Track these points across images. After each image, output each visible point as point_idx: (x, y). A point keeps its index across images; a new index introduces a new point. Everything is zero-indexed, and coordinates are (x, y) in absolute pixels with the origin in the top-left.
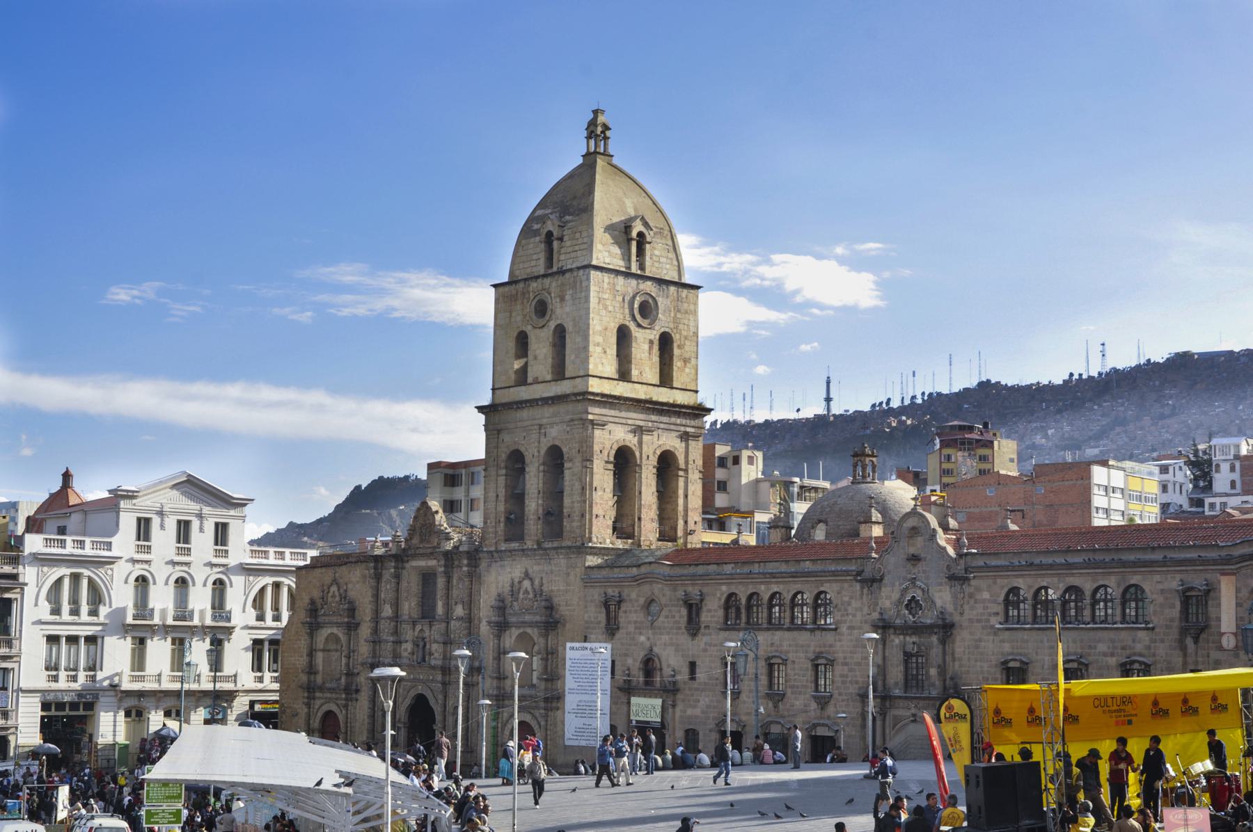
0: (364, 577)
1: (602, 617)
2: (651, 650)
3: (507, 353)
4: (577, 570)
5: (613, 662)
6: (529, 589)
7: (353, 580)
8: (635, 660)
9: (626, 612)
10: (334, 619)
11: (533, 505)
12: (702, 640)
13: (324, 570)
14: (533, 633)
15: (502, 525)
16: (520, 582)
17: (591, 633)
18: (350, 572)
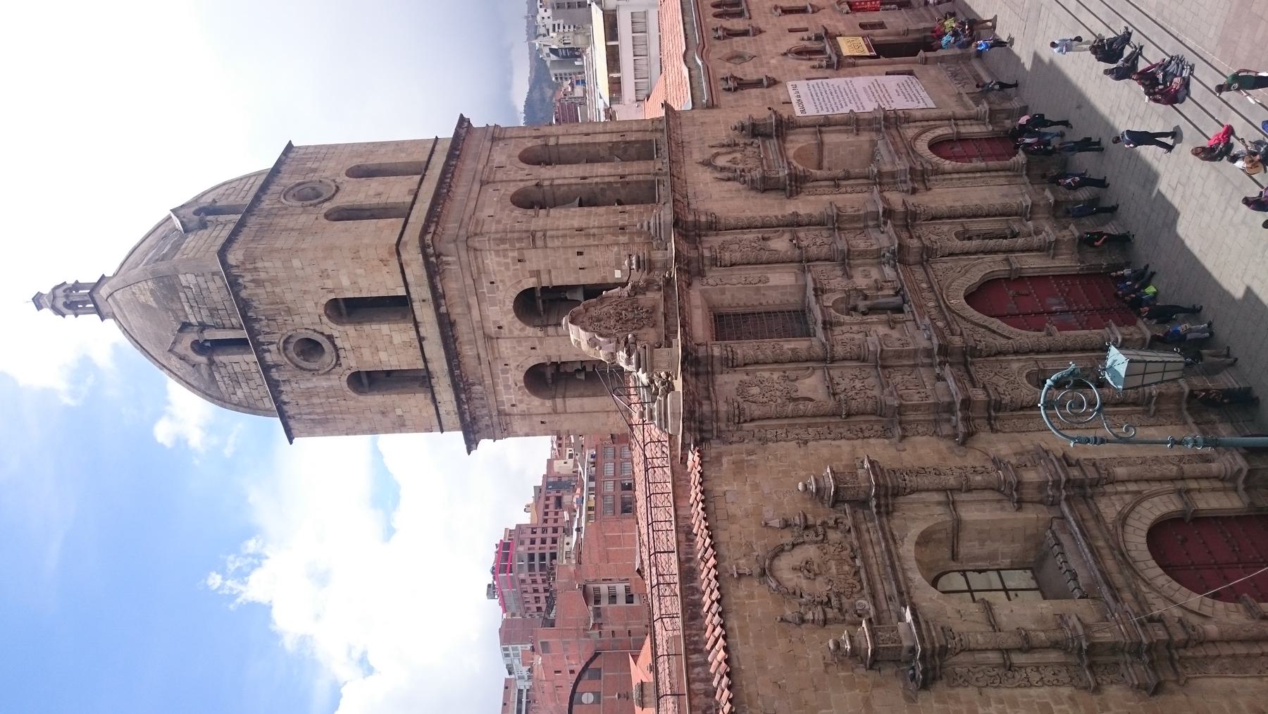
0: (739, 467)
1: (755, 92)
2: (785, 54)
3: (346, 230)
4: (696, 116)
5: (807, 79)
6: (730, 157)
7: (749, 502)
8: (802, 65)
9: (745, 75)
10: (876, 553)
11: (602, 172)
12: (762, 26)
13: (733, 623)
14: (793, 148)
15: (628, 208)
16: (722, 169)
17: (779, 99)
18: (730, 518)
